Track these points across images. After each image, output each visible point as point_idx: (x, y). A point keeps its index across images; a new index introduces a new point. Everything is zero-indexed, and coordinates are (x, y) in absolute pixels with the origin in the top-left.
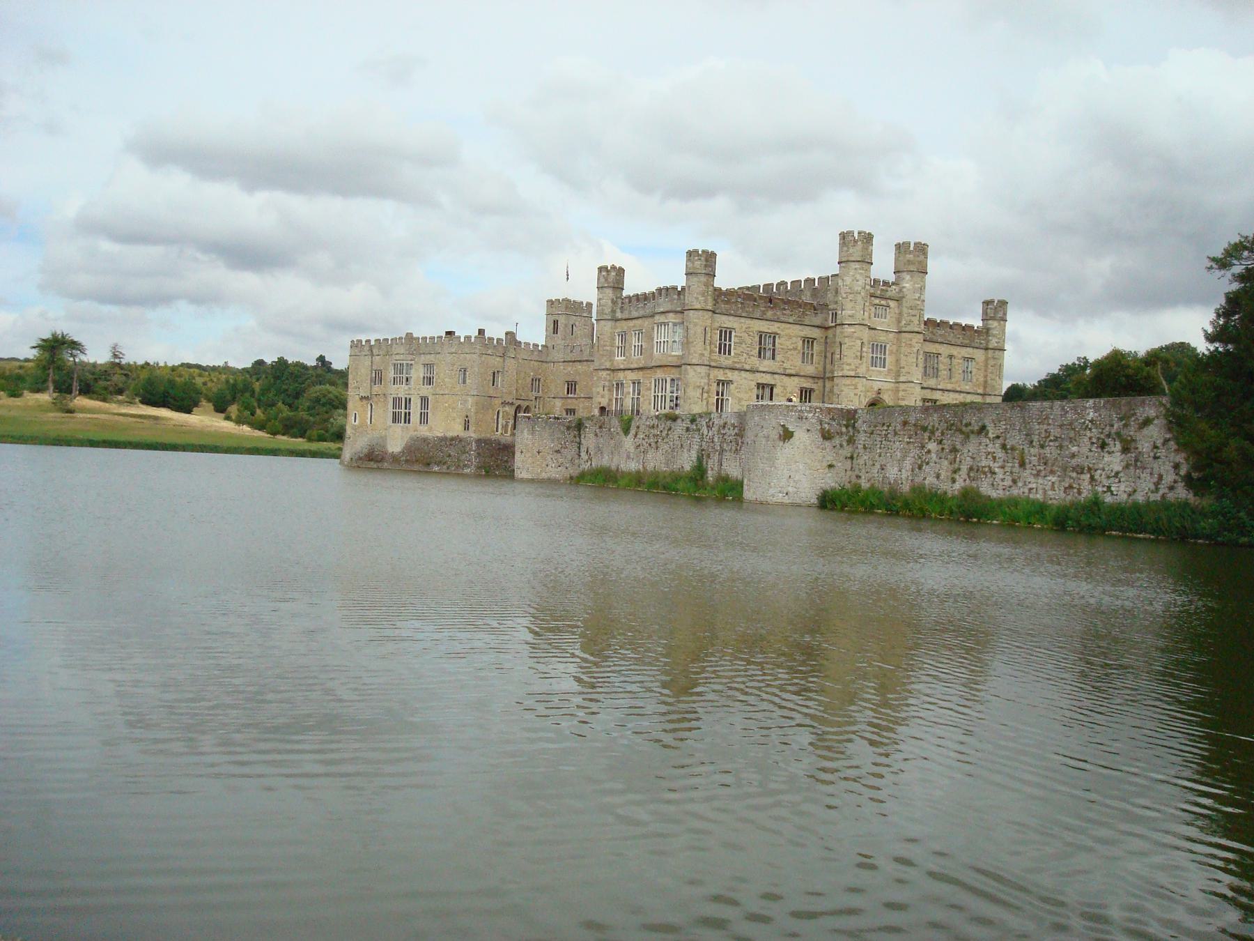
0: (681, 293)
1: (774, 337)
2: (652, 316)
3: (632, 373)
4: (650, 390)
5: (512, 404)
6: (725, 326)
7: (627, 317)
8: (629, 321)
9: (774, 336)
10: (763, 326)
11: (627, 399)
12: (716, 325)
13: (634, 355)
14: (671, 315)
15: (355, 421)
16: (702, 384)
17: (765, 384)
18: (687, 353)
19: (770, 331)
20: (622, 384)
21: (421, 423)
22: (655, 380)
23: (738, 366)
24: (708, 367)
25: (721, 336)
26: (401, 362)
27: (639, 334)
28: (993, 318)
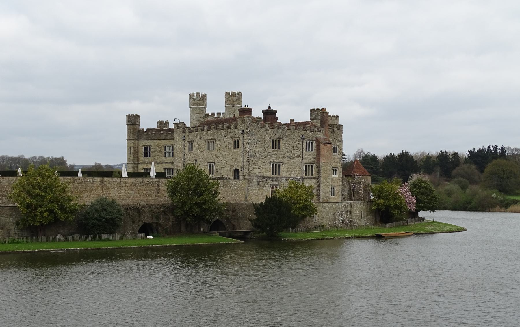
6: (146, 145)
10: (166, 142)
12: (142, 145)
19: (170, 144)
24: (133, 164)
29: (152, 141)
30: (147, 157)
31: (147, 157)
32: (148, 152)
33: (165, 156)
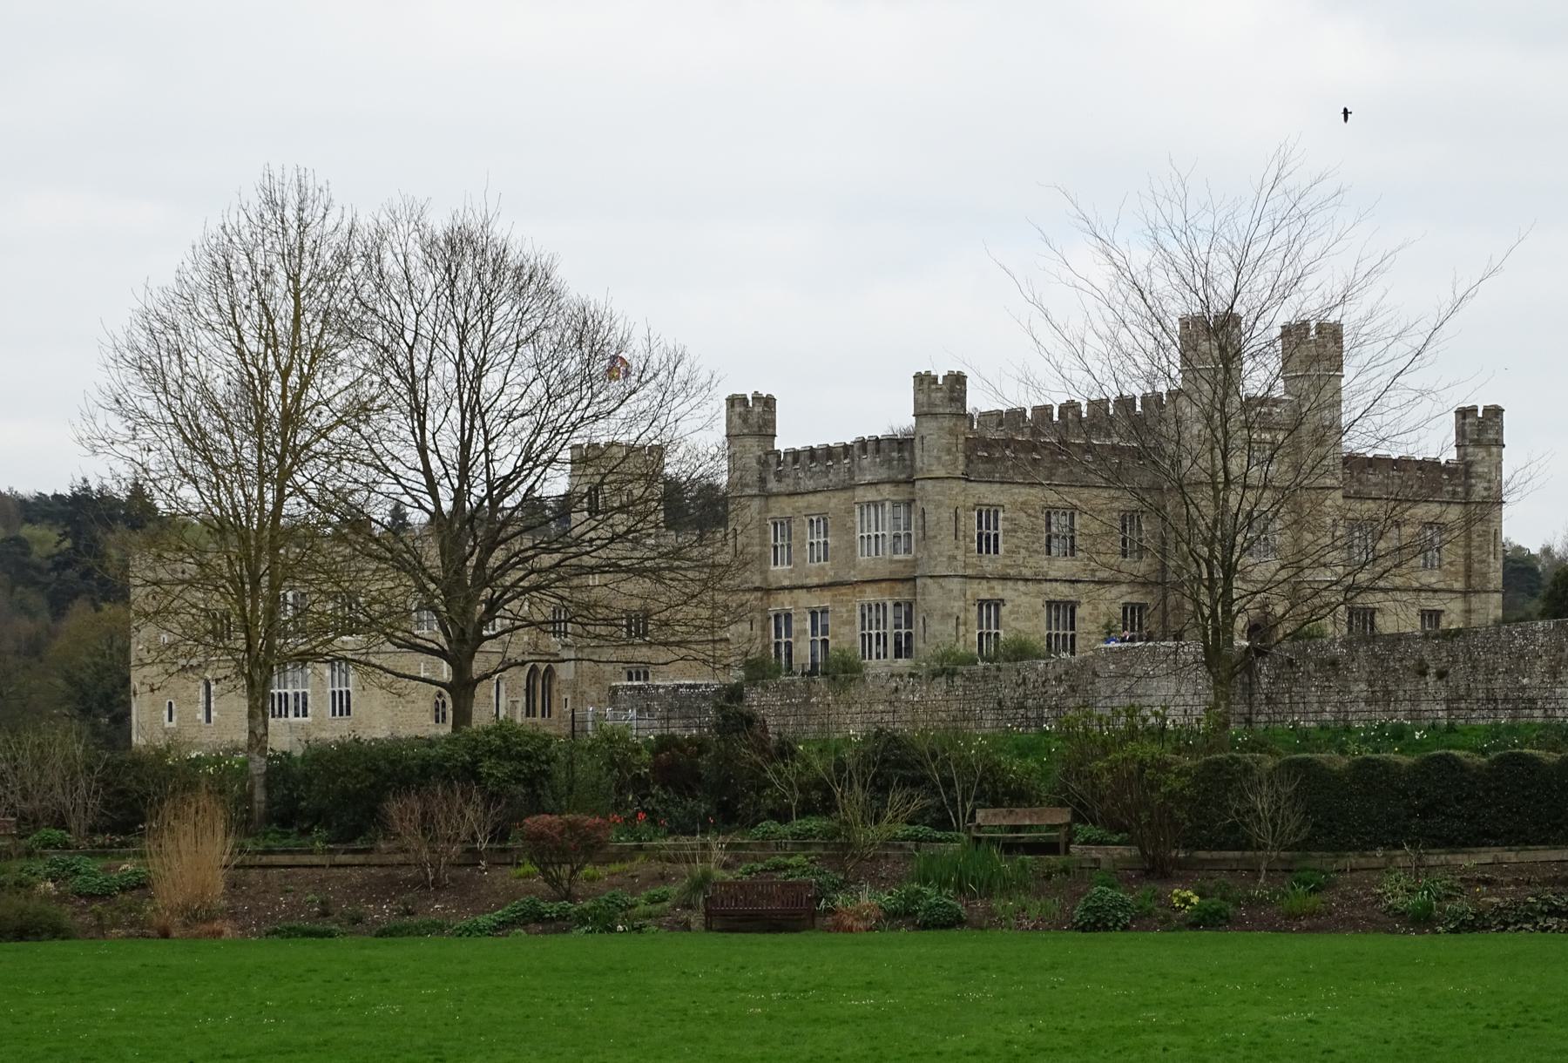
0: (902, 444)
1: (1072, 515)
2: (853, 487)
4: (853, 623)
5: (523, 663)
6: (986, 501)
8: (796, 498)
9: (1072, 511)
11: (800, 644)
12: (970, 503)
13: (811, 560)
14: (887, 490)
15: (170, 719)
16: (955, 610)
17: (1061, 602)
18: (926, 556)
20: (788, 616)
21: (334, 714)
22: (862, 606)
23: (1012, 572)
25: (980, 522)
27: (818, 521)
28: (1477, 443)
29: (1006, 486)
30: (988, 552)
31: (988, 552)
32: (992, 533)
33: (1049, 553)
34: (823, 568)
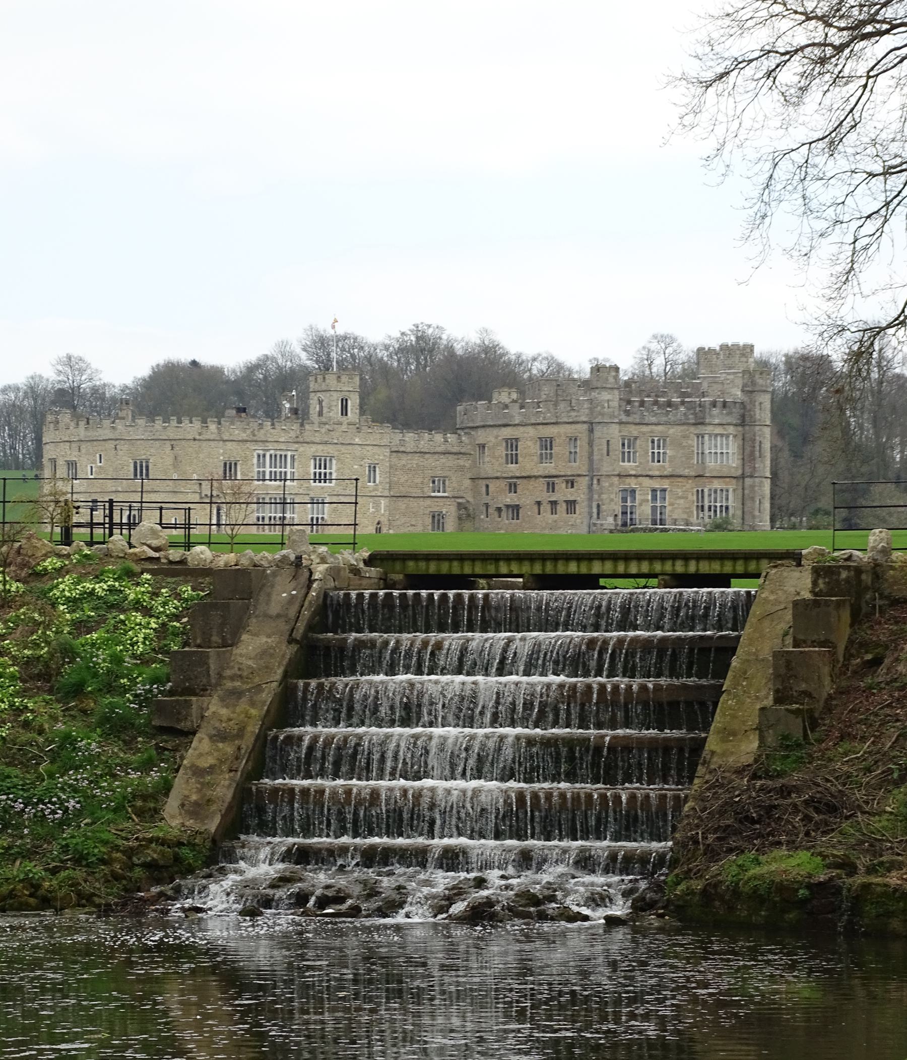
3: (651, 481)
7: (638, 421)
11: (643, 507)
13: (653, 461)
20: (633, 491)
26: (283, 453)
27: (659, 440)
34: (663, 467)
